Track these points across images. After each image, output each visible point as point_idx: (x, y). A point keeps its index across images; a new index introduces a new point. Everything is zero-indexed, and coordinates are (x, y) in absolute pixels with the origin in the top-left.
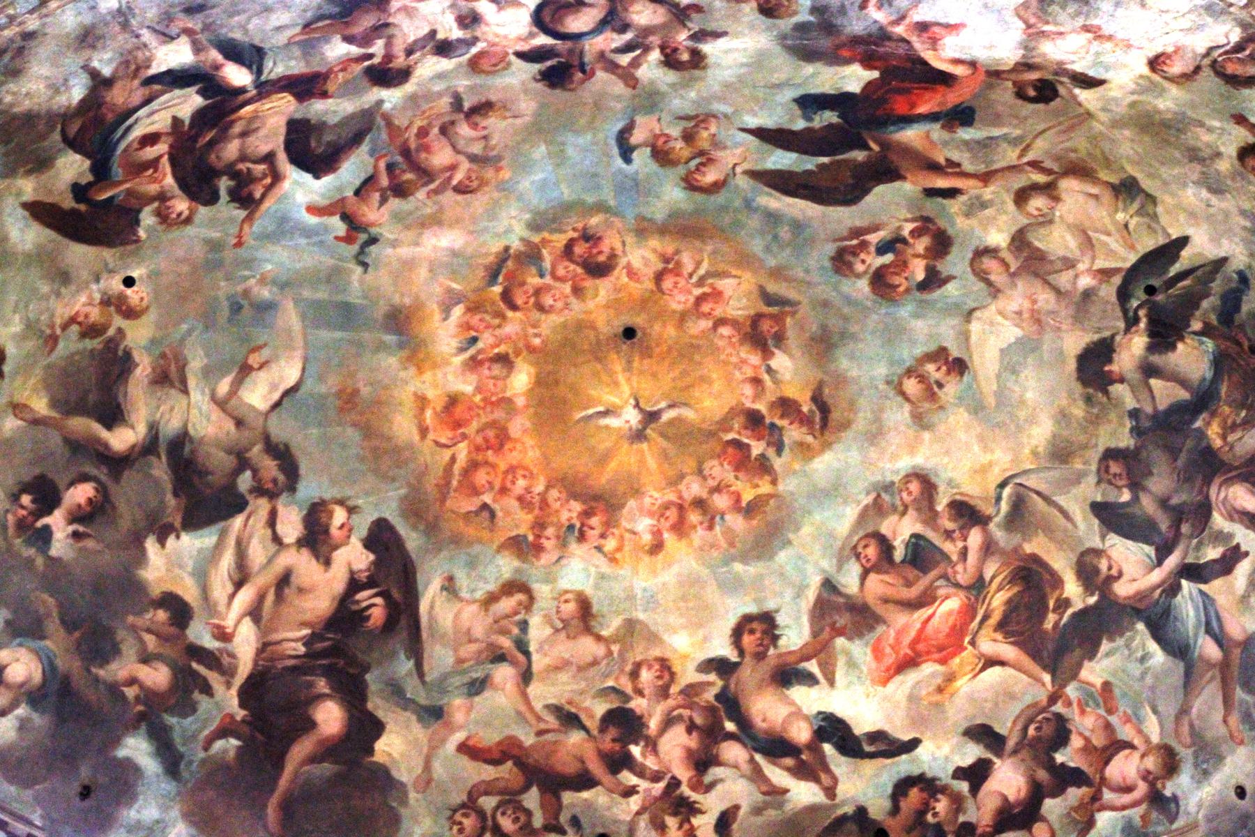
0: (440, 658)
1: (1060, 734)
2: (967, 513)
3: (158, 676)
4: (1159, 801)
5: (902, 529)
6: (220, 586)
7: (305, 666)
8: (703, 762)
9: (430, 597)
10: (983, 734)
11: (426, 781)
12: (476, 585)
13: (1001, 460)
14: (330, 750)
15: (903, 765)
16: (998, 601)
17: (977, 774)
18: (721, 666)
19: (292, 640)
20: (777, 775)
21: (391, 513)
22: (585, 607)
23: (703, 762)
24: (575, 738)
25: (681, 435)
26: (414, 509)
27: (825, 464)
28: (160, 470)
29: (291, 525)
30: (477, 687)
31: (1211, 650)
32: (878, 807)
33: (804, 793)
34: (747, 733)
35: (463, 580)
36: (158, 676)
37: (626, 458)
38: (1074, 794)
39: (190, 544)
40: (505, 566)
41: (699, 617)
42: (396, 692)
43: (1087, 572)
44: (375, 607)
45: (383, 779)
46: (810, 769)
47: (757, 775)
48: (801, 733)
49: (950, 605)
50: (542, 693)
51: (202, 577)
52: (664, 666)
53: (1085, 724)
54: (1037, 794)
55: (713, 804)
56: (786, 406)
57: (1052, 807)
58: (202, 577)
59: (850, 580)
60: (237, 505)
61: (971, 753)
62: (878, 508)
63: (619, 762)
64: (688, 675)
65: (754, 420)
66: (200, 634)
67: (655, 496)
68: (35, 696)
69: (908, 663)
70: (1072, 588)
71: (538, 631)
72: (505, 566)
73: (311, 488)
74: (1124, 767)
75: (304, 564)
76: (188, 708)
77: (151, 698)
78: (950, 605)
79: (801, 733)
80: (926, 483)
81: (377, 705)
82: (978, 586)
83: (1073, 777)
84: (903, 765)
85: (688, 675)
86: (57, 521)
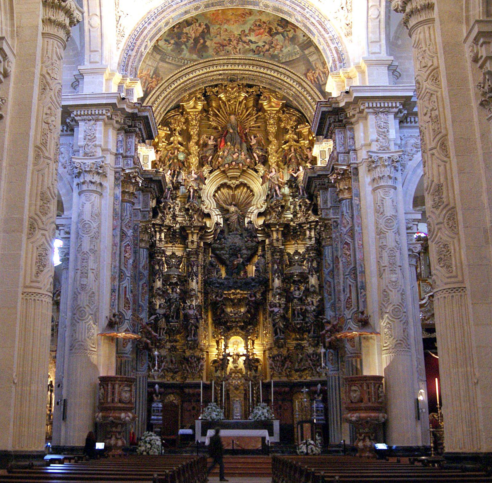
0: (212, 35)
1: (272, 43)
2: (264, 23)
3: (185, 40)
4: (281, 51)
5: (258, 23)
6: (191, 31)
7: (199, 37)
8: (237, 44)
9: (211, 30)
10: (264, 42)
11: (211, 46)
12: (215, 28)
13: (268, 19)
14: (201, 44)
15: (257, 45)
16: (267, 30)
17: (264, 46)
18: (240, 35)
19: (198, 35)
20: (245, 45)
21: (207, 22)
22: (226, 29)
23: (237, 44)
24: (225, 42)
25: (236, 15)
26: (209, 22)
27: (250, 18)
28: (185, 23)
29: (197, 25)
30: (216, 37)
31: (287, 37)
32: (254, 49)
33: (247, 47)
34: (242, 41)
35: (214, 28)
36: (185, 40)
37: (230, 17)
38: (273, 49)
39: (188, 28)
40: (219, 26)
41: (237, 30)
42: (208, 38)
43: (276, 29)
44: (206, 31)
45: (207, 46)
46: (248, 45)
47: (243, 45)
48: (247, 41)
49: (262, 30)
50: (222, 38)
51: (189, 30)
52: (234, 35)
53: (275, 42)
54: (270, 48)
55: (238, 48)
56: (247, 13)
57: (271, 50)
58: (189, 30)
59: (252, 27)
60: (192, 24)
61: (264, 44)
62: (256, 21)
63: (229, 44)
64: (236, 35)
65: (243, 14)
66: (189, 35)
67: (233, 20)
68: (174, 44)
69: (257, 35)
70: (274, 30)
71: (222, 32)
72: (219, 26)
73: (199, 22)
74: (278, 47)
75: (199, 28)
76: (188, 42)
77: (185, 42)
78: (262, 30)
79: (247, 41)
80: (261, 20)
81: (206, 40)
82: (265, 29)
83: (274, 47)
84: (257, 45)
85: (236, 35)
86: (175, 29)
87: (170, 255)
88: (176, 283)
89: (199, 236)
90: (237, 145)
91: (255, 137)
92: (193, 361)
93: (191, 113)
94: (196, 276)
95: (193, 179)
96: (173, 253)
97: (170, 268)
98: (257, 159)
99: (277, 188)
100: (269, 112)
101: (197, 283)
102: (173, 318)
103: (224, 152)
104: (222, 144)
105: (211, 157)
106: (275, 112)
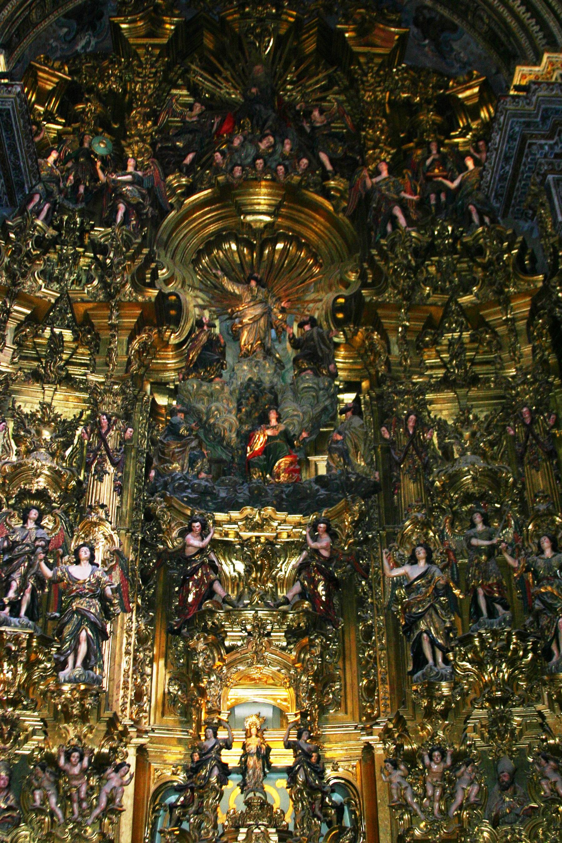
87: (33, 415)
88: (41, 495)
89: (136, 345)
90: (270, 123)
91: (321, 113)
92: (76, 770)
93: (141, 51)
94: (114, 464)
95: (129, 178)
96: (46, 406)
97: (29, 452)
98: (329, 167)
99: (397, 211)
100: (362, 60)
101: (119, 489)
102: (15, 612)
103: (230, 142)
104: (226, 127)
105: (190, 156)
106: (378, 61)
